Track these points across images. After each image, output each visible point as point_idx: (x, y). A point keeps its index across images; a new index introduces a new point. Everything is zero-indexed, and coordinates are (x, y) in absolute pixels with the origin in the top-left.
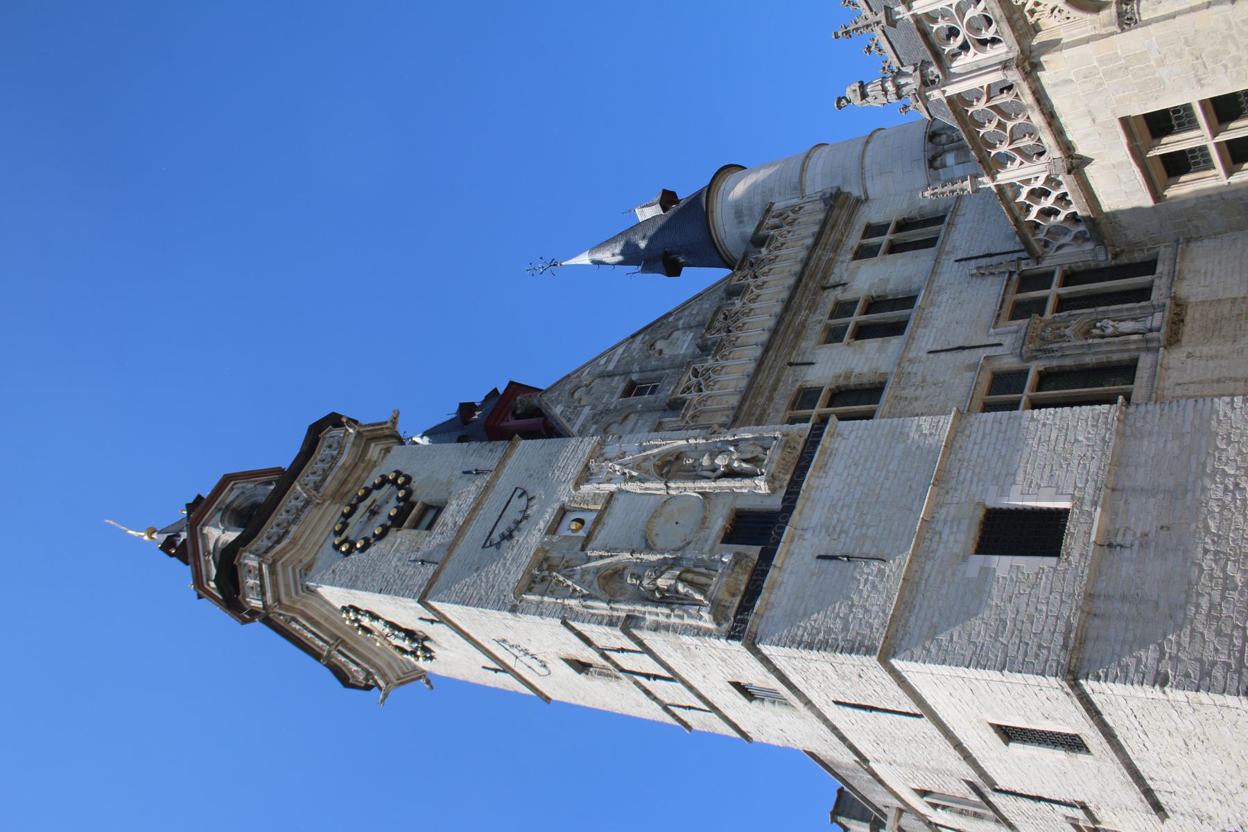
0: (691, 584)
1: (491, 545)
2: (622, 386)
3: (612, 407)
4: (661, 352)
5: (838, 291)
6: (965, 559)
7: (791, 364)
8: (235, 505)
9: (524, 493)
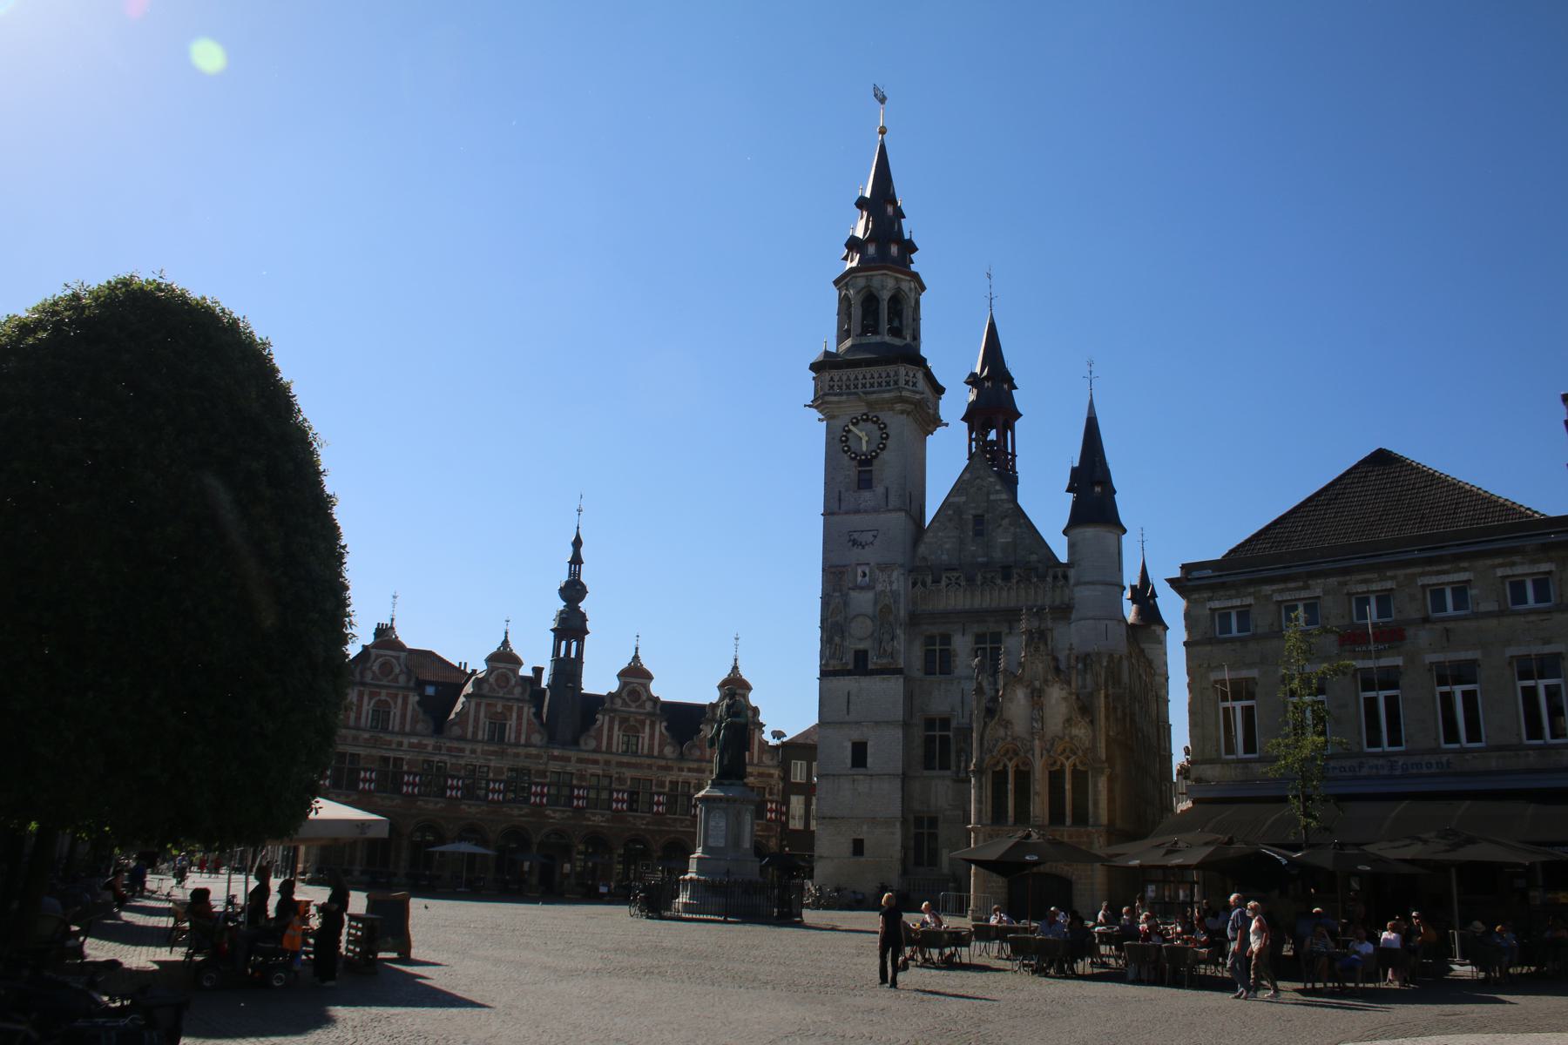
0: (836, 648)
2: (979, 512)
3: (964, 517)
4: (1000, 525)
5: (1007, 631)
6: (850, 740)
7: (964, 624)
9: (875, 536)
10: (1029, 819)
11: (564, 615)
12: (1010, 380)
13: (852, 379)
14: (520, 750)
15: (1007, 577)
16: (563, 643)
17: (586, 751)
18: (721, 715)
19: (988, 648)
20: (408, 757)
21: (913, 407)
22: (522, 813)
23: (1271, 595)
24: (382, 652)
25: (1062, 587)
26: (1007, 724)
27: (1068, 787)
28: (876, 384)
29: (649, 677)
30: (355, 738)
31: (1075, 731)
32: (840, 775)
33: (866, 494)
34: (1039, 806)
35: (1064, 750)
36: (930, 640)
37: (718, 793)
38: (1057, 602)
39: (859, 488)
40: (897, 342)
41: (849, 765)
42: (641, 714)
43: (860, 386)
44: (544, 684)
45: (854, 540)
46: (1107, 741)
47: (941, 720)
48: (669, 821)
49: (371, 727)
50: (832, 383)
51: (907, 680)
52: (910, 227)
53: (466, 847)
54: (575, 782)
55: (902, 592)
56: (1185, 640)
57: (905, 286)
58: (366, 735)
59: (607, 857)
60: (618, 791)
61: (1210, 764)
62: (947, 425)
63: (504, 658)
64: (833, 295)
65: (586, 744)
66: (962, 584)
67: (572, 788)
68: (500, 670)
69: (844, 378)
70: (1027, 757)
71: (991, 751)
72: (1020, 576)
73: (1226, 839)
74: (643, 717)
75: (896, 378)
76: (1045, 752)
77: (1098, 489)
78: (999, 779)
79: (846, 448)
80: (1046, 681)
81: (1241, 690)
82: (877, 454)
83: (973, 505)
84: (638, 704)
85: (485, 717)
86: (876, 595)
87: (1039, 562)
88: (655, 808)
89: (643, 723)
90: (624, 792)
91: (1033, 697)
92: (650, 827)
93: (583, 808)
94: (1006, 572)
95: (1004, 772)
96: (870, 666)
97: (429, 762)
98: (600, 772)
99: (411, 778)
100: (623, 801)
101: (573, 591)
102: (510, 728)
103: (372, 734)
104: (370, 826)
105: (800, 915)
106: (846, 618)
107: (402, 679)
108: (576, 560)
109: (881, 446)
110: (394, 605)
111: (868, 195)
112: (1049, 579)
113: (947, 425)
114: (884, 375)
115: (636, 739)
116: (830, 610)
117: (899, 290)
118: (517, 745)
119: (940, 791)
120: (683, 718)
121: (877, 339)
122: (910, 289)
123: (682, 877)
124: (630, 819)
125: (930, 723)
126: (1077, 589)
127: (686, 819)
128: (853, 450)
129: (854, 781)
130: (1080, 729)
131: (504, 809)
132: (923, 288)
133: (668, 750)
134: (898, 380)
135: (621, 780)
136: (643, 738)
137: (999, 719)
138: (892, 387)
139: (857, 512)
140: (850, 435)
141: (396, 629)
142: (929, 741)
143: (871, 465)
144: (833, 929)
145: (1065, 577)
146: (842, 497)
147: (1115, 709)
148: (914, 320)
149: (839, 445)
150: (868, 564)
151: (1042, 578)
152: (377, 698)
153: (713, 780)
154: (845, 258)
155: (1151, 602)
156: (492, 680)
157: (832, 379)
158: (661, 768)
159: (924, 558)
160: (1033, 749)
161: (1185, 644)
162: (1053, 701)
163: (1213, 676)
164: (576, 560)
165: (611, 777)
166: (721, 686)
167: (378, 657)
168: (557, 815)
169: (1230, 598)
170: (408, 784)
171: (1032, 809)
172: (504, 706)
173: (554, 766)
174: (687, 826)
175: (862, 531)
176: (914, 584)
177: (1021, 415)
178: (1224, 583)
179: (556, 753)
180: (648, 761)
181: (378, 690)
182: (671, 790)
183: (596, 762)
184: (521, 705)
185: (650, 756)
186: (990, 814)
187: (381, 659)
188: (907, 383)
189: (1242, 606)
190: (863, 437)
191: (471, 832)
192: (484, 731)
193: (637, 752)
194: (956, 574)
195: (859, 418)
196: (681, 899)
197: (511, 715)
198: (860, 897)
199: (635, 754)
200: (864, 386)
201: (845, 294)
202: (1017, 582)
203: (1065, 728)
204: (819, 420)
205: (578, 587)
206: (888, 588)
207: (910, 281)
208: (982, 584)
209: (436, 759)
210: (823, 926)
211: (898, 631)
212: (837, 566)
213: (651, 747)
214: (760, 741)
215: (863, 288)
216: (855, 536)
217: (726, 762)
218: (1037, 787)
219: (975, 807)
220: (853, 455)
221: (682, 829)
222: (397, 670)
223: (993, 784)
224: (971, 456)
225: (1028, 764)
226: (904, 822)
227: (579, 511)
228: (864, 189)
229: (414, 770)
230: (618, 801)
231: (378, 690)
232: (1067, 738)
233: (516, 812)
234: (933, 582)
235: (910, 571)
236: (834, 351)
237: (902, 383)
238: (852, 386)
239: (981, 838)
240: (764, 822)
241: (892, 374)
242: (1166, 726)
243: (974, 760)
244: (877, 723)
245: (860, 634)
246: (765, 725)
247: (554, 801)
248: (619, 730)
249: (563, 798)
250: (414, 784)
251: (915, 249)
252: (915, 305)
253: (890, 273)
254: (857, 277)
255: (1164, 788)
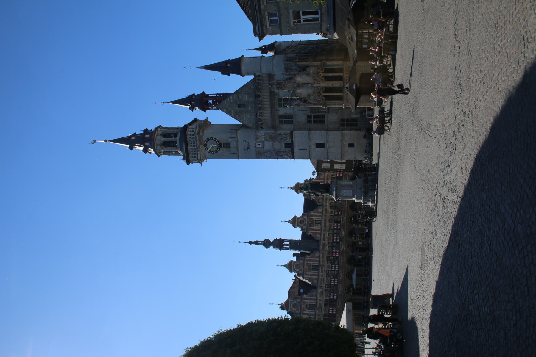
1: (246, 150)
2: (237, 106)
4: (241, 99)
7: (276, 111)
8: (161, 143)
10: (341, 88)
11: (275, 246)
12: (191, 96)
13: (192, 150)
14: (321, 260)
15: (259, 96)
16: (285, 246)
17: (321, 238)
18: (308, 193)
19: (284, 102)
20: (324, 297)
21: (201, 129)
22: (342, 259)
23: (264, 5)
24: (289, 307)
25: (262, 77)
26: (309, 95)
27: (330, 75)
28: (194, 142)
29: (295, 217)
30: (319, 315)
31: (311, 72)
32: (327, 152)
33: (232, 144)
34: (337, 84)
35: (318, 76)
36: (281, 122)
37: (334, 193)
38: (267, 79)
39: (230, 147)
40: (179, 135)
41: (324, 149)
42: (308, 220)
43: (194, 147)
44: (298, 252)
45: (247, 148)
46: (314, 62)
47: (308, 118)
48: (344, 209)
49: (315, 310)
50: (194, 157)
51: (295, 130)
52: (139, 131)
53: (354, 277)
54: (331, 241)
55: (265, 132)
56: (280, 35)
57: (160, 132)
58: (317, 312)
59: (356, 230)
60: (334, 227)
61: (322, 26)
62: (207, 117)
63: (290, 266)
64: (163, 157)
65: (318, 238)
66: (261, 111)
67: (333, 242)
68: (294, 267)
69: (192, 153)
70: (320, 89)
71: (318, 101)
72: (259, 92)
73: (347, 21)
74: (309, 219)
75: (191, 135)
76: (318, 83)
77: (229, 65)
78: (327, 98)
79: (216, 152)
80: (294, 82)
81: (297, 15)
82: (218, 141)
83: (235, 108)
84: (304, 221)
85: (309, 272)
86: (266, 141)
87: (254, 85)
88: (339, 214)
89: (311, 219)
90: (334, 225)
91: (300, 87)
92: (346, 215)
93: (340, 238)
94: (257, 96)
95: (325, 96)
96: (290, 142)
97: (326, 290)
98: (328, 233)
99: (331, 296)
100: (337, 225)
101: (267, 244)
102: (314, 263)
103: (317, 310)
104: (348, 309)
105: (374, 164)
106: (274, 151)
107: (298, 300)
108: (256, 243)
109: (215, 140)
110: (273, 304)
111: (128, 146)
112: (260, 82)
113: (207, 117)
114: (190, 139)
115: (317, 222)
116: (270, 156)
117: (161, 135)
118: (319, 261)
119: (332, 118)
120: (309, 205)
121: (178, 142)
122: (161, 130)
123: (362, 204)
124: (343, 223)
125: (309, 122)
126: (263, 73)
127: (343, 204)
128: (216, 149)
129: (329, 147)
130: (311, 71)
131: (341, 265)
132: (160, 126)
133: (320, 210)
134: (192, 134)
135: (330, 226)
136: (316, 219)
137: (307, 98)
138: (195, 136)
139: (237, 148)
140: (211, 151)
141: (281, 303)
142: (315, 122)
143: (222, 143)
144: (379, 153)
145: (259, 76)
146: (233, 153)
147: (304, 59)
148: (171, 129)
149: (215, 154)
150: (255, 143)
151: (259, 84)
152: (305, 308)
153: (330, 195)
154: (150, 153)
155: (267, 47)
156: (298, 270)
157: (192, 157)
158: (326, 212)
159: (253, 124)
160: (317, 87)
161: (281, 35)
162: (301, 80)
163: (292, 25)
164: (256, 243)
165: (329, 229)
166: (298, 193)
167: (291, 309)
168: (343, 247)
169: (265, 20)
170: (333, 297)
171: (338, 87)
172: (306, 266)
173: (326, 248)
174: (345, 203)
175: (244, 146)
176: (262, 128)
177: (203, 92)
178: (260, 22)
179: (322, 248)
180: (324, 217)
181: (302, 308)
182: (333, 209)
183: (324, 234)
184: (306, 260)
185: (322, 216)
186: (340, 101)
187: (292, 308)
188: (193, 131)
189: (268, 16)
190: (212, 146)
191: (349, 276)
192: (315, 272)
193: (321, 221)
194: (258, 114)
195: (205, 147)
196: (370, 205)
197: (309, 263)
198: (368, 145)
199: (321, 221)
200: (194, 146)
201: (163, 153)
202: (261, 92)
203: (310, 76)
204: (206, 161)
205: (265, 242)
206: (264, 136)
207: (158, 131)
208: (262, 105)
209: (325, 288)
210: (378, 157)
211: (278, 133)
212: (256, 154)
213: (319, 216)
214: (316, 179)
215: (160, 146)
216: (246, 148)
217: (323, 190)
218: (330, 85)
219: (337, 106)
220: (218, 149)
221: (346, 205)
222: (295, 302)
223: (329, 100)
224: (218, 109)
225: (322, 88)
226: (343, 130)
227: (239, 242)
228: (126, 147)
229: (329, 295)
230: (337, 227)
231: (302, 308)
232: (314, 75)
233: (342, 261)
234: (261, 121)
235: (258, 129)
236: (183, 156)
237: (193, 133)
238: (195, 150)
239: (347, 104)
240: (343, 177)
241: (190, 136)
242: (309, 41)
243: (322, 107)
244: (309, 140)
245: (279, 146)
246: (311, 178)
247: (338, 248)
248: (313, 227)
249: (337, 245)
250: (333, 295)
251: (147, 129)
252: (166, 129)
253: (155, 138)
254: (157, 149)
255: (330, 42)
